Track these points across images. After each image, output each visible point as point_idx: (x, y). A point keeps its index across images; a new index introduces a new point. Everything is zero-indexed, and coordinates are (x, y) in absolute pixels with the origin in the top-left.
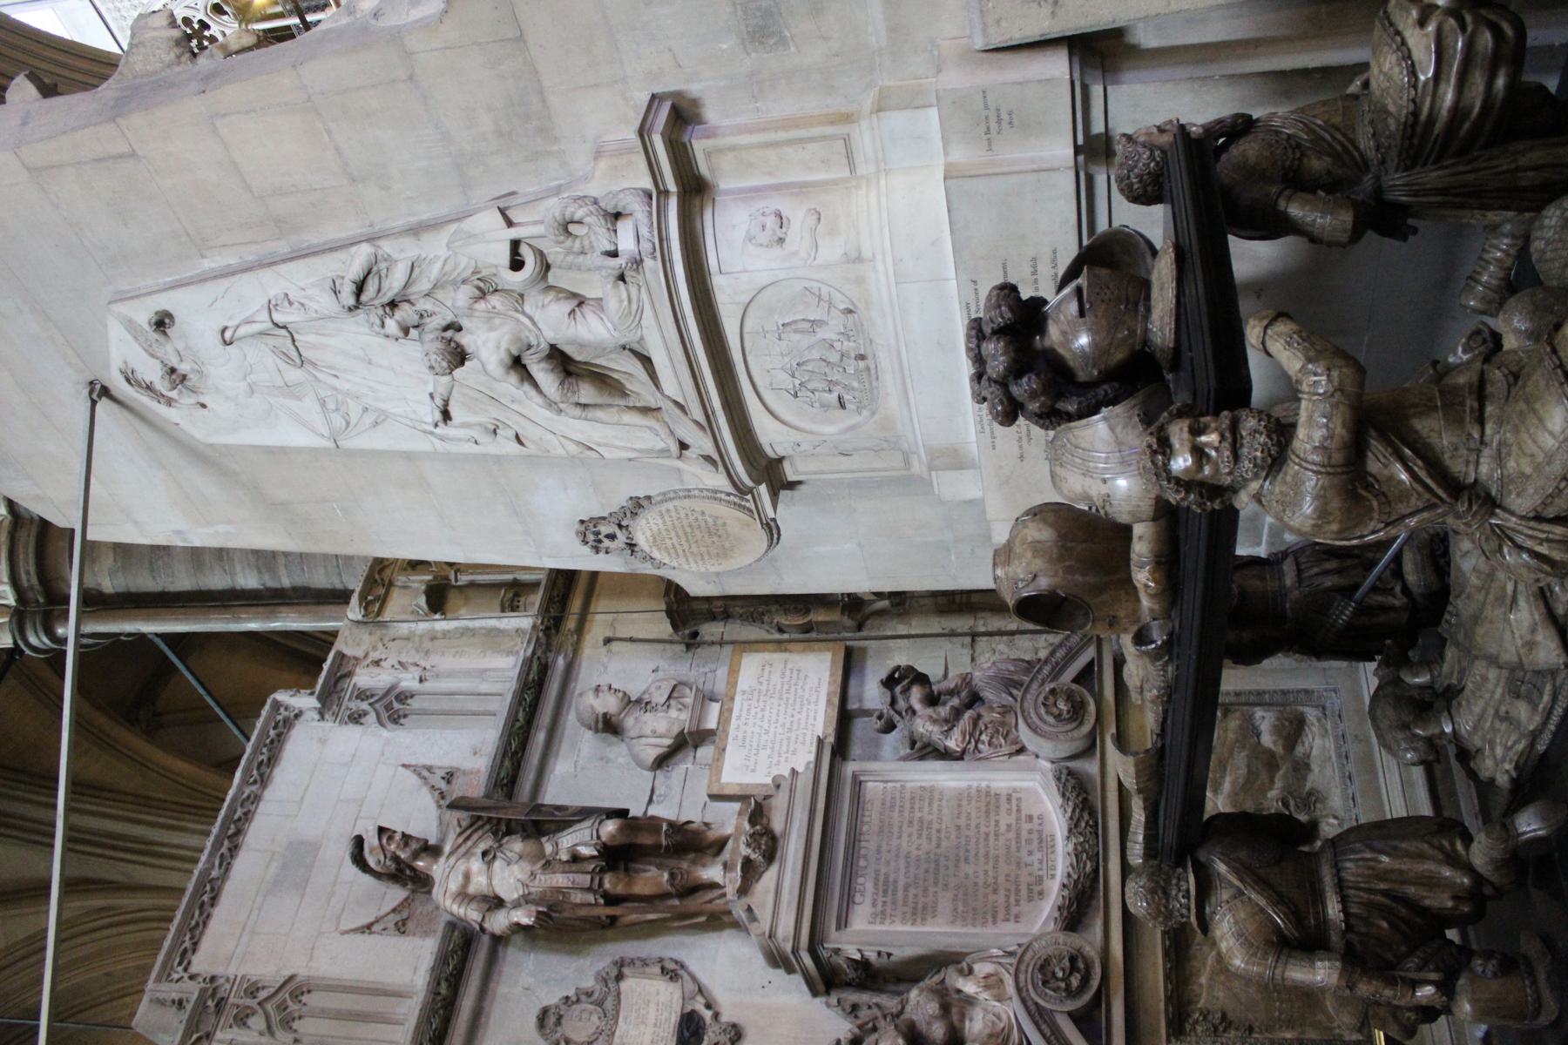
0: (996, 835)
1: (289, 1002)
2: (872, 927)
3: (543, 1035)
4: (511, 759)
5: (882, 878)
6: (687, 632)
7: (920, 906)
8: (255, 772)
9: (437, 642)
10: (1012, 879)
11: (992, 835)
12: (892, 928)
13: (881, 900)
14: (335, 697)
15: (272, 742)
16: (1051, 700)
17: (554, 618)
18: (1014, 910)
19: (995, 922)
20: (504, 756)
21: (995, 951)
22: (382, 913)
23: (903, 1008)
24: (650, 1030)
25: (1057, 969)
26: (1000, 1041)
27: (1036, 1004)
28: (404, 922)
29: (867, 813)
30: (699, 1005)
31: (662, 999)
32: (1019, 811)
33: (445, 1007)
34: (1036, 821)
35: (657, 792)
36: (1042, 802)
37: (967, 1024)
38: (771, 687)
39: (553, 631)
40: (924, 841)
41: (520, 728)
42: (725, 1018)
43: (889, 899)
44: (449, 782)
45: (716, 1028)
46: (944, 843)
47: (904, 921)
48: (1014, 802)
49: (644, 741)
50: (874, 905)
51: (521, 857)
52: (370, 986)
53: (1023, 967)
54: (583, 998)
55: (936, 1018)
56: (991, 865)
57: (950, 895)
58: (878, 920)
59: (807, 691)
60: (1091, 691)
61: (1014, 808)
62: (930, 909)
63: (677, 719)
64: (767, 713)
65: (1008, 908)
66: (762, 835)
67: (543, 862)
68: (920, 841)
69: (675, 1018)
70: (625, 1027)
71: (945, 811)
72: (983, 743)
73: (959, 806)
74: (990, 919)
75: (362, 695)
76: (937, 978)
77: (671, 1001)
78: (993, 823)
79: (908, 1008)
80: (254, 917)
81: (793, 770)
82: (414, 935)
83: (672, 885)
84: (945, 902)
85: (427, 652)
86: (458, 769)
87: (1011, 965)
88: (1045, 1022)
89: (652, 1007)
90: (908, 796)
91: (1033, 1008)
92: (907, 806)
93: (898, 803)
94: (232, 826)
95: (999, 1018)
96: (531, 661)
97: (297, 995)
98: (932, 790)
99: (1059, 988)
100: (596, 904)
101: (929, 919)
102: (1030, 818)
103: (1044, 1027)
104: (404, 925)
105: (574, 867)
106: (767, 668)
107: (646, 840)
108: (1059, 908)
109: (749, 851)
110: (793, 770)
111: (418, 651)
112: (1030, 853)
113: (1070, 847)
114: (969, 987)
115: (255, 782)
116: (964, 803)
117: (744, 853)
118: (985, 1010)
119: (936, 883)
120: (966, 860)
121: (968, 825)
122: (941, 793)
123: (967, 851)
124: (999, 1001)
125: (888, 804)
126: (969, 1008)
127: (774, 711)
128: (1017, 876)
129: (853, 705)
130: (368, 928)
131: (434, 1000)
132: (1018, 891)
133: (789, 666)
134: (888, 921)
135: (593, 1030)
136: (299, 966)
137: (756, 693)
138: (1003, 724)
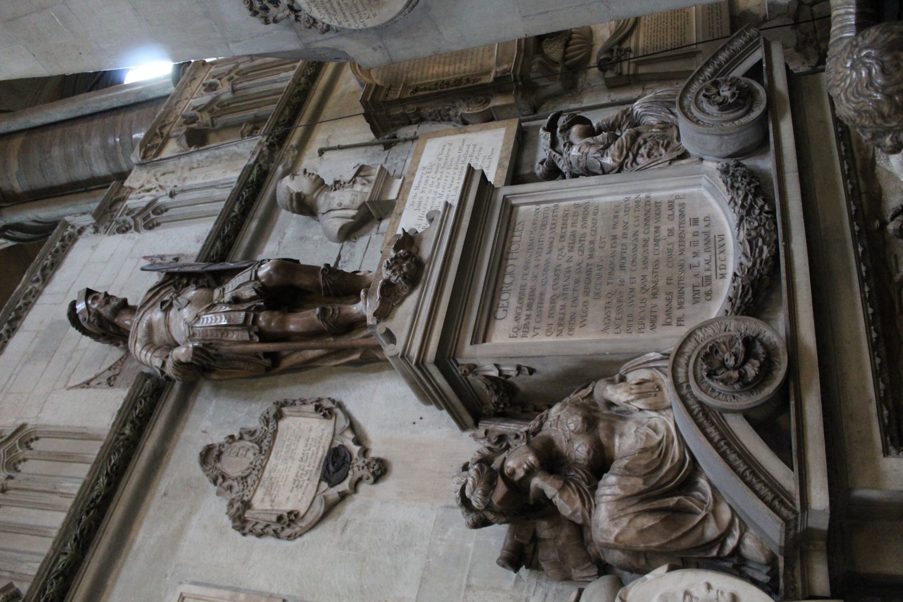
0: (657, 241)
1: (17, 446)
2: (512, 341)
3: (204, 471)
4: (223, 241)
5: (527, 291)
6: (387, 137)
7: (567, 318)
8: (39, 273)
9: (194, 171)
10: (675, 280)
11: (652, 241)
12: (536, 340)
13: (524, 313)
14: (109, 214)
15: (57, 251)
16: (714, 90)
17: (278, 137)
18: (677, 313)
19: (653, 327)
21: (652, 355)
22: (100, 371)
23: (541, 425)
24: (297, 463)
25: (727, 356)
26: (655, 456)
27: (701, 403)
28: (115, 376)
29: (516, 234)
30: (348, 440)
31: (313, 435)
32: (682, 215)
33: (127, 447)
34: (702, 223)
35: (342, 259)
36: (709, 204)
37: (617, 441)
38: (449, 161)
39: (277, 147)
40: (575, 255)
41: (235, 217)
42: (373, 454)
43: (534, 312)
45: (360, 463)
46: (597, 253)
47: (548, 333)
48: (677, 208)
49: (332, 214)
50: (517, 319)
51: (189, 302)
52: (77, 431)
53: (682, 361)
54: (246, 437)
55: (578, 433)
56: (650, 270)
57: (602, 302)
58: (520, 333)
59: (481, 159)
60: (762, 84)
61: (677, 213)
62: (578, 319)
63: (361, 192)
64: (442, 182)
65: (669, 313)
66: (405, 258)
68: (569, 254)
69: (321, 452)
71: (600, 223)
72: (642, 156)
73: (616, 217)
74: (648, 325)
75: (130, 212)
76: (584, 392)
77: (322, 435)
78: (652, 229)
79: (547, 424)
80: (11, 381)
81: (447, 204)
82: (119, 387)
83: (323, 320)
84: (596, 312)
85: (185, 179)
86: (183, 255)
87: (666, 367)
88: (712, 424)
89: (302, 441)
90: (560, 213)
91: (696, 408)
92: (560, 222)
93: (550, 221)
94: (13, 313)
95: (655, 430)
96: (253, 168)
97: (26, 443)
98: (586, 207)
99: (731, 378)
100: (251, 341)
101: (577, 329)
102: (695, 221)
103: (710, 430)
104: (115, 379)
105: (234, 307)
106: (447, 148)
107: (305, 281)
108: (730, 299)
109: (389, 272)
110: (447, 204)
111: (179, 179)
112: (696, 255)
113: (743, 234)
114: (618, 395)
115: (38, 280)
116: (622, 214)
118: (639, 423)
119: (587, 293)
120: (622, 267)
121: (624, 234)
122: (597, 208)
123: (624, 258)
124: (656, 411)
125: (539, 223)
126: (621, 422)
127: (450, 179)
128: (681, 279)
129: (526, 171)
130: (88, 384)
131: (117, 439)
132: (681, 293)
133: (466, 143)
134: (531, 333)
135: (247, 465)
136: (32, 418)
137: (434, 168)
138: (664, 137)
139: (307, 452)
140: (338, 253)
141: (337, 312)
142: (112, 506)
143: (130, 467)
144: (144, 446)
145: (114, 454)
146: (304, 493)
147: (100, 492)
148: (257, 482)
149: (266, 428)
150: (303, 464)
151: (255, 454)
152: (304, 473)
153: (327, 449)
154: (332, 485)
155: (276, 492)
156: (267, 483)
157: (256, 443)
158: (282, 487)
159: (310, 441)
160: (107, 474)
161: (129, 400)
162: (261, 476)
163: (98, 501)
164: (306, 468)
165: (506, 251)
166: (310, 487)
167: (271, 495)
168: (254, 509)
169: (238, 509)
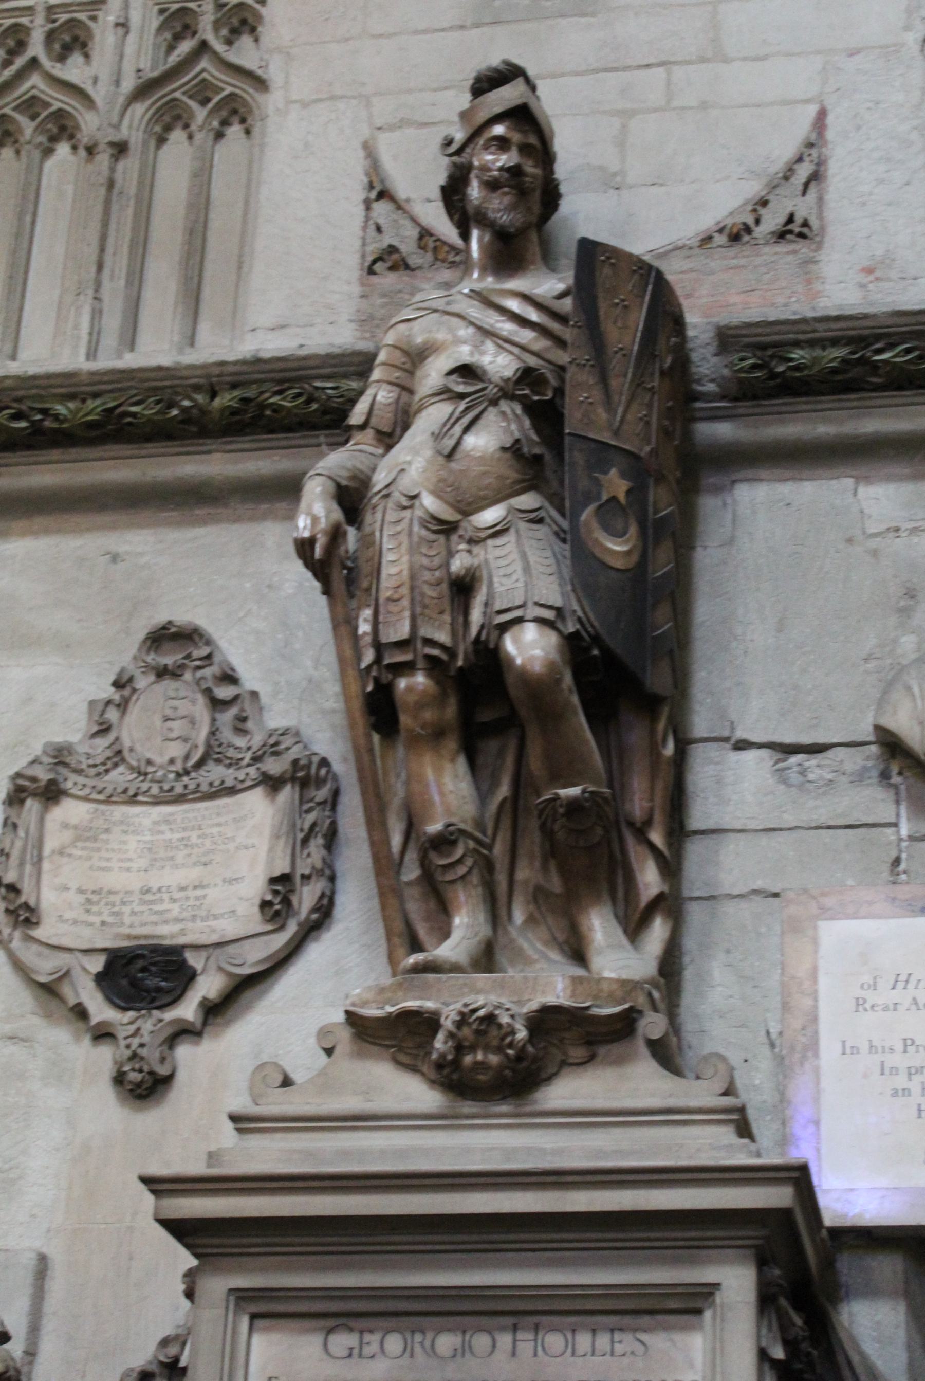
20: (850, 341)
24: (134, 882)
29: (603, 1340)
33: (187, 418)
35: (812, 762)
44: (782, 235)
67: (448, 514)
70: (147, 822)
77: (215, 917)
104: (392, 268)
117: (445, 1011)
131: (197, 388)
139: (166, 896)
140: (835, 740)
141: (450, 876)
142: (55, 454)
143: (151, 448)
144: (209, 452)
145: (158, 402)
146: (75, 922)
147: (66, 420)
148: (101, 797)
149: (247, 760)
150: (136, 897)
151: (172, 761)
152: (116, 909)
153: (181, 941)
154: (101, 979)
155: (79, 853)
156: (100, 823)
157: (209, 746)
158: (88, 864)
159: (199, 892)
160: (110, 411)
161: (295, 365)
162: (115, 803)
163: (48, 424)
164: (127, 910)
165: (545, 1319)
166: (87, 932)
167: (73, 844)
168: (46, 809)
169: (34, 779)
